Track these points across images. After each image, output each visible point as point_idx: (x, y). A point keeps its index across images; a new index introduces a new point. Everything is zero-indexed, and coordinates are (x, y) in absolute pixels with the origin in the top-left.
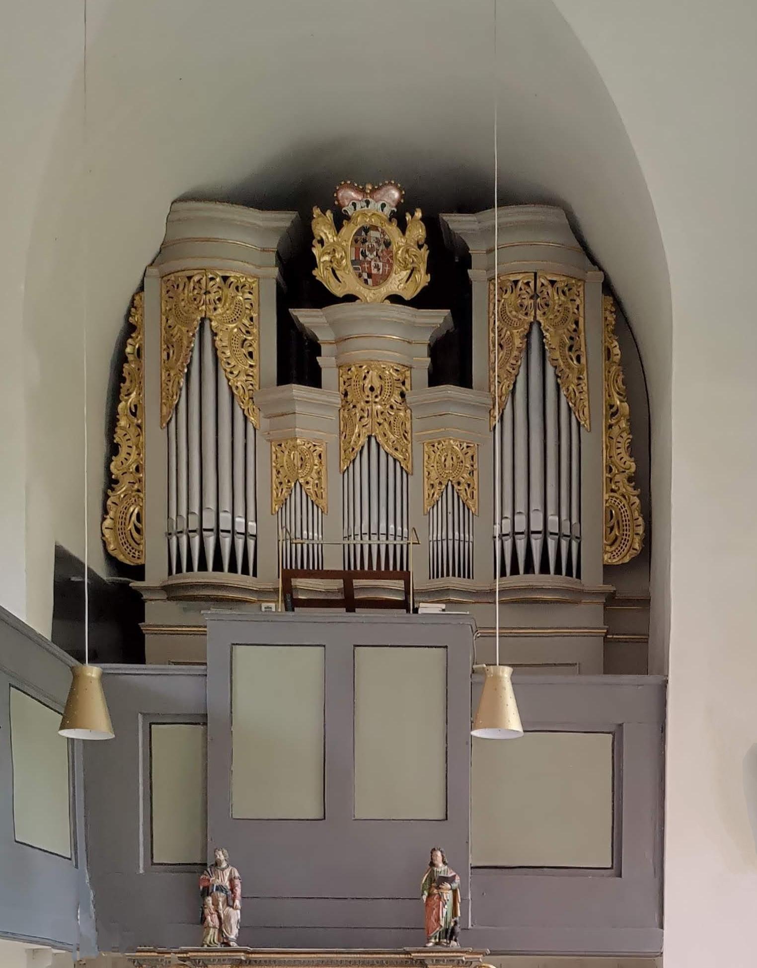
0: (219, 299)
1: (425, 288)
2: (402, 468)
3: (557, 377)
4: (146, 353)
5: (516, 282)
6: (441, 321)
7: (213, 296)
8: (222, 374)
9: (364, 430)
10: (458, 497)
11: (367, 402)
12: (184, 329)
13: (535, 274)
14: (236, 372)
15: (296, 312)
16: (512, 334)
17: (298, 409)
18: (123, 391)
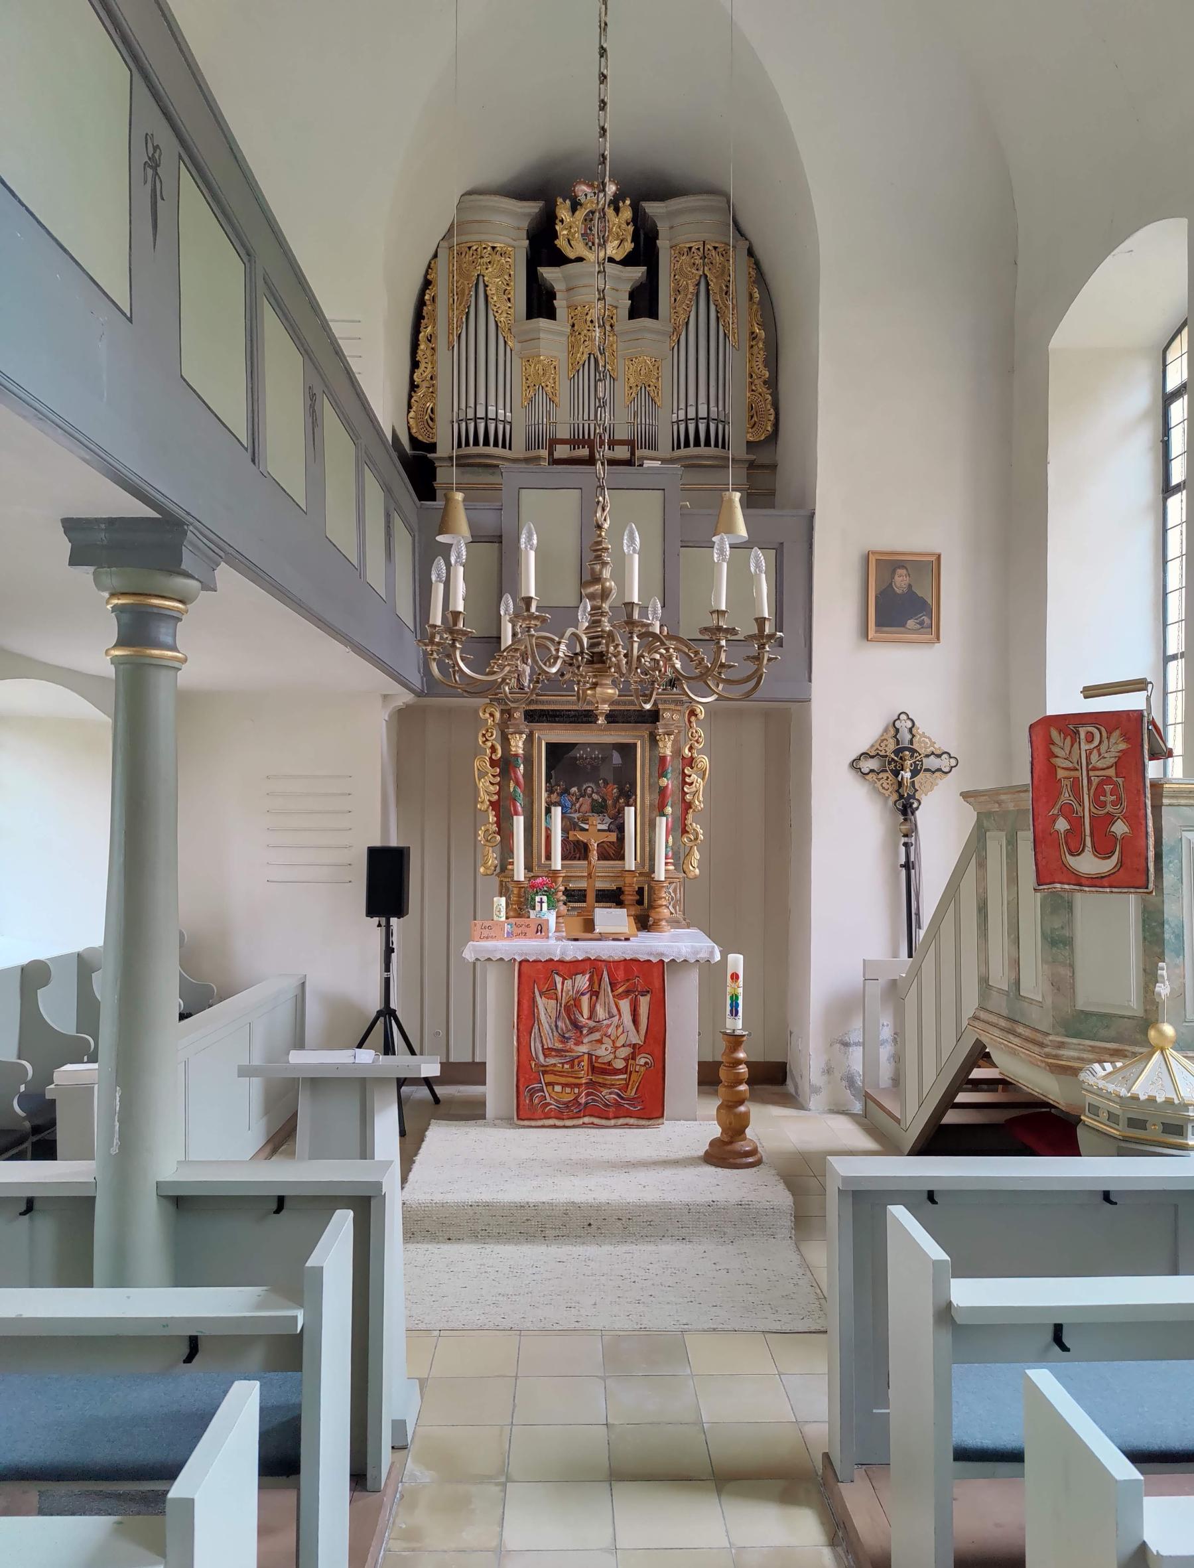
0: (490, 262)
1: (630, 252)
2: (610, 376)
3: (718, 312)
4: (439, 300)
5: (690, 248)
6: (640, 274)
7: (485, 260)
8: (491, 313)
9: (586, 350)
10: (649, 394)
11: (589, 330)
12: (466, 282)
13: (704, 242)
14: (500, 312)
15: (541, 270)
16: (687, 284)
17: (542, 335)
18: (423, 326)
